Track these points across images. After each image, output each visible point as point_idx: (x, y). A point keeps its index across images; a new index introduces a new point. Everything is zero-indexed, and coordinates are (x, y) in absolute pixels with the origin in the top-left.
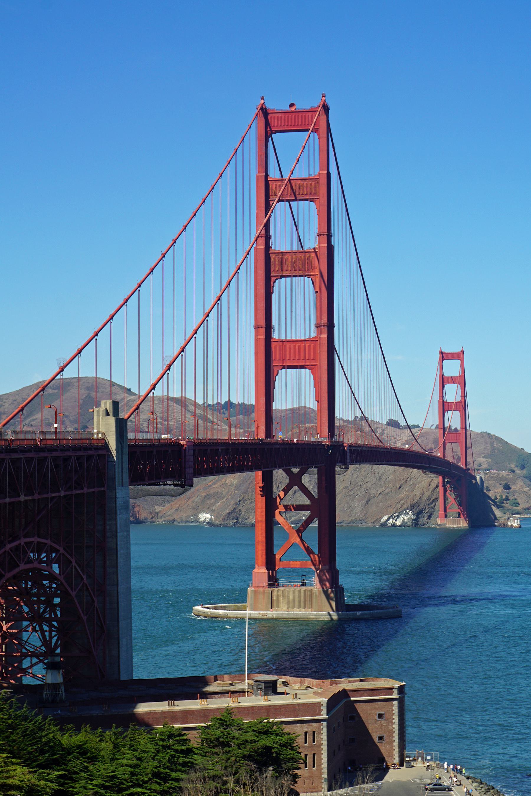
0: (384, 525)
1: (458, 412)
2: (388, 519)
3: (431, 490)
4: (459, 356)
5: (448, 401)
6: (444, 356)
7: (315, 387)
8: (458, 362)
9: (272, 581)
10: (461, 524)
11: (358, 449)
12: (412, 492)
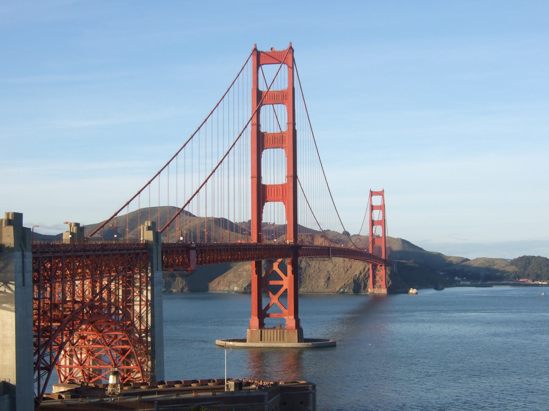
0: (338, 292)
2: (340, 289)
3: (365, 271)
4: (381, 193)
5: (375, 220)
6: (372, 193)
7: (286, 212)
8: (381, 197)
9: (262, 325)
11: (314, 248)
12: (354, 273)
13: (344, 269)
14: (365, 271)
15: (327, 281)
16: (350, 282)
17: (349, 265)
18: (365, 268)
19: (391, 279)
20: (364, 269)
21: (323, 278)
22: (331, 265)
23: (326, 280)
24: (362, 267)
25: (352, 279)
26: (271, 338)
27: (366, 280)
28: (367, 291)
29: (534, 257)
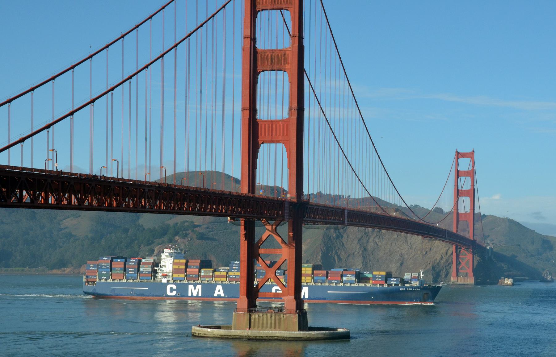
1: (469, 197)
6: (459, 155)
8: (469, 160)
10: (469, 281)
14: (448, 255)
15: (400, 266)
16: (428, 267)
20: (447, 253)
24: (444, 249)
25: (431, 265)
26: (263, 324)
28: (450, 281)
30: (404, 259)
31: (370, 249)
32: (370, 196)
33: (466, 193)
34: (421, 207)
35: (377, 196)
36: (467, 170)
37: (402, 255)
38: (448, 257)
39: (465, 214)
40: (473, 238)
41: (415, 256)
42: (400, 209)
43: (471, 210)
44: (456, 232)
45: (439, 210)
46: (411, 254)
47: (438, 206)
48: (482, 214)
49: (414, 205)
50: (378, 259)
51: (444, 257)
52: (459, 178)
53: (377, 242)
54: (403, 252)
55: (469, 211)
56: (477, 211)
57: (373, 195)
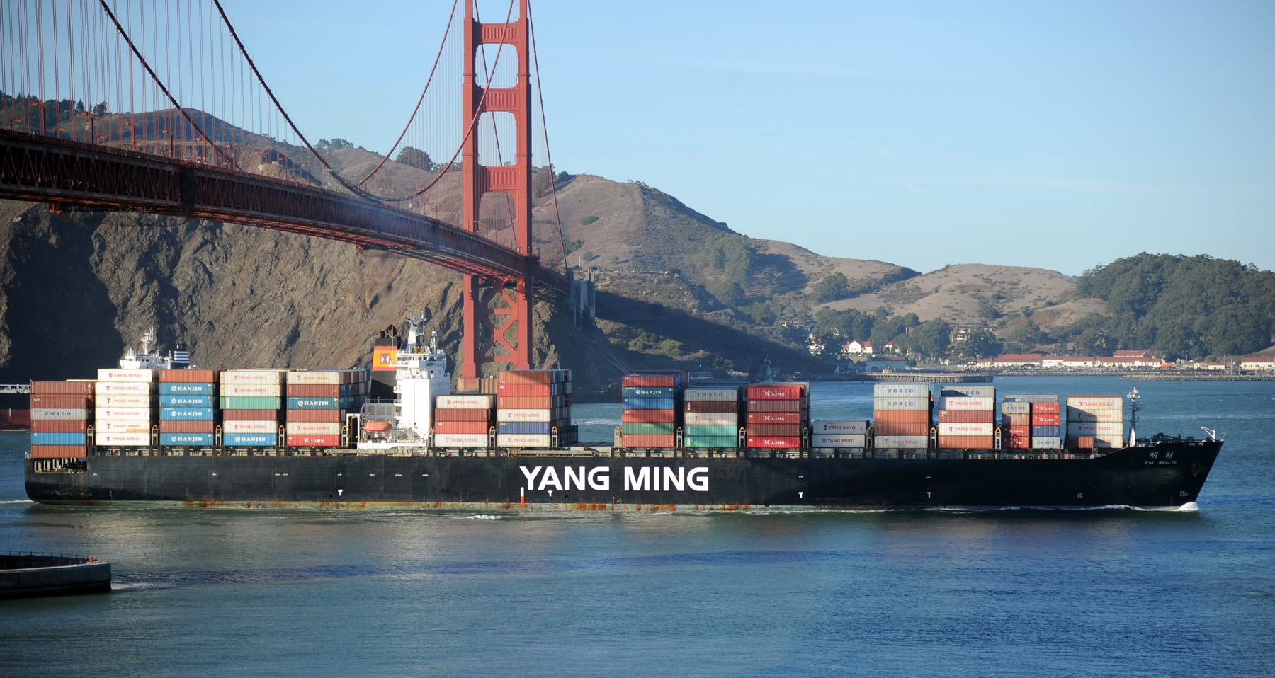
3: (448, 306)
13: (359, 298)
14: (448, 306)
17: (384, 281)
18: (445, 292)
19: (553, 340)
21: (272, 337)
22: (304, 278)
23: (284, 341)
27: (451, 345)
29: (1177, 260)
30: (298, 321)
31: (181, 288)
32: (173, 106)
33: (505, 100)
34: (356, 146)
35: (198, 107)
36: (504, 22)
37: (293, 306)
38: (449, 313)
39: (506, 170)
40: (530, 250)
41: (338, 312)
42: (284, 152)
43: (519, 155)
44: (471, 230)
45: (416, 159)
46: (324, 304)
47: (415, 141)
48: (557, 172)
49: (330, 142)
50: (211, 323)
51: (436, 312)
52: (480, 47)
53: (208, 266)
54: (297, 297)
55: (514, 162)
56: (539, 162)
57: (185, 105)
